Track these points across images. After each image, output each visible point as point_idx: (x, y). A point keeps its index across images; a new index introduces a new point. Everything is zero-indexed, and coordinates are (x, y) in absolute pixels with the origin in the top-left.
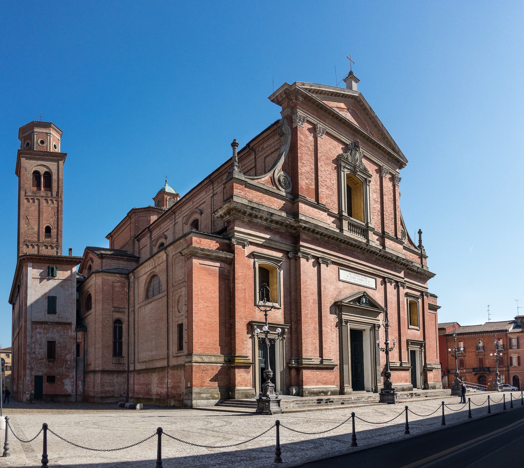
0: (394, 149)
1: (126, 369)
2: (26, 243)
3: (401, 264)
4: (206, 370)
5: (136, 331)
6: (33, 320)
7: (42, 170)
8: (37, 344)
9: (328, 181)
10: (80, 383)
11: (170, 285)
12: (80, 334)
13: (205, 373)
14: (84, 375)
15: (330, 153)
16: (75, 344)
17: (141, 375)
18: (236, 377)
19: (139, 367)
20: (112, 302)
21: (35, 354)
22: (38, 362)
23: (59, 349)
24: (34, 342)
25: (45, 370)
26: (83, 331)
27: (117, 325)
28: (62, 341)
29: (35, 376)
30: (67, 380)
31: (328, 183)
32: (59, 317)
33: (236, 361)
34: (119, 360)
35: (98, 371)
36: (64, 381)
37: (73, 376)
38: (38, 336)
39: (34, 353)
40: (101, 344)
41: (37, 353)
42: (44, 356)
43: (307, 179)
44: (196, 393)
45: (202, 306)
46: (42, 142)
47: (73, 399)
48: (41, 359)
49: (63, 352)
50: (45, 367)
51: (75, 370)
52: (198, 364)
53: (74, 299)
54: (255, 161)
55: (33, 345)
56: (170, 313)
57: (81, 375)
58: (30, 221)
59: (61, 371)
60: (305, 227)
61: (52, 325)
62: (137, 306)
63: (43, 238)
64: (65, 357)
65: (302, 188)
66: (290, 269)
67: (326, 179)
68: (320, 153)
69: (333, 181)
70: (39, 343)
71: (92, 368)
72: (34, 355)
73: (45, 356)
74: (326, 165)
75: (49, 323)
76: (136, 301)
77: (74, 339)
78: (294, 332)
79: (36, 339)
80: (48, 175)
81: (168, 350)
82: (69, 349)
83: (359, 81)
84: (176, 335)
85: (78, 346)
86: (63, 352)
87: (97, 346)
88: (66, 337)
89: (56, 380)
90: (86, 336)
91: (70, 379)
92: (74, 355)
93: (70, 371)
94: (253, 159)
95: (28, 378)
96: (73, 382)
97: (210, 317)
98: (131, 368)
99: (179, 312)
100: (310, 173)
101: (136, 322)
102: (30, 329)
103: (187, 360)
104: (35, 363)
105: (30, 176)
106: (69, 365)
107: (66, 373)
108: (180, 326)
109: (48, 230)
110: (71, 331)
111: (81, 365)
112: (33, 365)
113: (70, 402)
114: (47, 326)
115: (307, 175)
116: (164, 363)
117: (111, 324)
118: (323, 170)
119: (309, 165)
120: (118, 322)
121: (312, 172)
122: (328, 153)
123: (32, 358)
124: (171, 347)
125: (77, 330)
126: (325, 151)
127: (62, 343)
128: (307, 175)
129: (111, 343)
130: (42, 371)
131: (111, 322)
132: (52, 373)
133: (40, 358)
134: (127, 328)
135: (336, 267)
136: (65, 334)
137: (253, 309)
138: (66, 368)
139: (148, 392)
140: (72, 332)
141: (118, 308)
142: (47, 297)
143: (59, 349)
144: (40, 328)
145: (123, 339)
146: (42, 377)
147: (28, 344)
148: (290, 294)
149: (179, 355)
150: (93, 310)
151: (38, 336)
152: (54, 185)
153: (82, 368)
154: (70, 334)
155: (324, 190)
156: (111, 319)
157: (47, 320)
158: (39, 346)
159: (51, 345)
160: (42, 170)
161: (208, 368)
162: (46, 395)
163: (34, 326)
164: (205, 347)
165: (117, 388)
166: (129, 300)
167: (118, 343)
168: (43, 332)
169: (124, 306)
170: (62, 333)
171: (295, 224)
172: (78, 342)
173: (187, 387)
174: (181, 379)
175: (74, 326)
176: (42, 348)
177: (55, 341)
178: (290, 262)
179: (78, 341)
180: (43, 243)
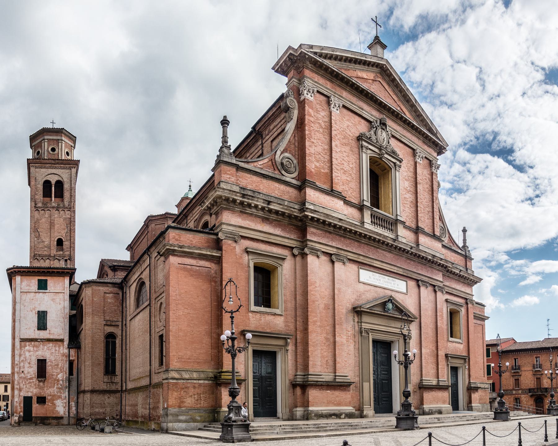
1: (120, 389)
2: (36, 257)
4: (186, 388)
5: (128, 346)
6: (22, 337)
7: (53, 179)
8: (27, 363)
9: (346, 164)
10: (73, 404)
11: (153, 291)
12: (73, 352)
13: (185, 391)
14: (78, 396)
15: (348, 131)
16: (68, 362)
17: (131, 395)
18: (223, 396)
19: (130, 386)
20: (103, 314)
21: (24, 374)
22: (28, 382)
23: (50, 367)
24: (23, 361)
25: (34, 391)
26: (76, 348)
27: (110, 340)
28: (54, 359)
29: (24, 397)
30: (59, 400)
31: (346, 167)
32: (50, 334)
33: (223, 377)
34: (111, 378)
35: (88, 391)
36: (56, 402)
37: (65, 397)
38: (27, 354)
39: (23, 372)
40: (91, 361)
41: (26, 372)
42: (34, 376)
43: (318, 161)
44: (172, 415)
45: (182, 313)
46: (53, 150)
47: (65, 421)
48: (31, 379)
49: (55, 371)
50: (35, 387)
51: (67, 390)
52: (175, 381)
53: (67, 314)
54: (262, 147)
55: (22, 364)
56: (153, 323)
57: (74, 396)
58: (41, 234)
59: (52, 391)
60: (313, 218)
61: (42, 341)
62: (129, 318)
63: (54, 252)
64: (57, 376)
65: (311, 172)
66: (295, 269)
67: (343, 162)
68: (335, 130)
70: (29, 361)
71: (82, 388)
72: (23, 375)
73: (35, 376)
74: (343, 145)
75: (39, 340)
76: (128, 312)
77: (66, 356)
79: (25, 358)
80: (59, 184)
81: (150, 365)
82: (61, 367)
84: (158, 349)
85: (71, 363)
86: (55, 371)
87: (87, 363)
88: (58, 355)
89: (47, 401)
90: (79, 353)
91: (62, 400)
92: (66, 373)
93: (62, 391)
94: (260, 145)
95: (16, 399)
96: (65, 403)
97: (191, 325)
98: (124, 388)
99: (161, 322)
100: (322, 154)
101: (128, 336)
102: (18, 347)
103: (164, 377)
104: (24, 383)
105: (40, 186)
106: (61, 385)
107: (57, 393)
108: (161, 337)
109: (60, 242)
110: (63, 348)
111: (74, 384)
112: (21, 385)
113: (63, 425)
114: (37, 343)
115: (317, 157)
116: (145, 382)
117: (102, 338)
118: (338, 150)
119: (321, 144)
120: (110, 338)
121: (324, 153)
122: (346, 131)
123: (21, 378)
124: (153, 362)
125: (69, 348)
126: (342, 129)
127: (53, 361)
128: (317, 157)
129: (103, 360)
130: (32, 391)
131: (103, 337)
132: (42, 393)
133: (29, 377)
134: (121, 343)
136: (57, 352)
137: (246, 316)
138: (58, 388)
139: (136, 415)
140: (64, 349)
141: (111, 321)
142: (37, 312)
143: (50, 367)
144: (29, 345)
145: (117, 356)
146: (31, 398)
147: (16, 362)
148: (295, 298)
149: (160, 371)
150: (84, 324)
151: (27, 354)
152: (66, 194)
153: (75, 388)
154: (62, 352)
155: (339, 175)
156: (103, 334)
157: (37, 337)
158: (28, 365)
159: (42, 364)
160: (53, 179)
161: (189, 385)
162: (36, 417)
163: (23, 343)
164: (185, 362)
165: (108, 409)
166: (122, 312)
167: (110, 360)
168: (32, 350)
169: (117, 319)
170: (54, 351)
171: (300, 214)
172: (71, 360)
173: (164, 408)
174: (160, 398)
175: (66, 343)
176: (32, 367)
177: (46, 360)
178: (295, 260)
179: (71, 358)
180: (54, 256)
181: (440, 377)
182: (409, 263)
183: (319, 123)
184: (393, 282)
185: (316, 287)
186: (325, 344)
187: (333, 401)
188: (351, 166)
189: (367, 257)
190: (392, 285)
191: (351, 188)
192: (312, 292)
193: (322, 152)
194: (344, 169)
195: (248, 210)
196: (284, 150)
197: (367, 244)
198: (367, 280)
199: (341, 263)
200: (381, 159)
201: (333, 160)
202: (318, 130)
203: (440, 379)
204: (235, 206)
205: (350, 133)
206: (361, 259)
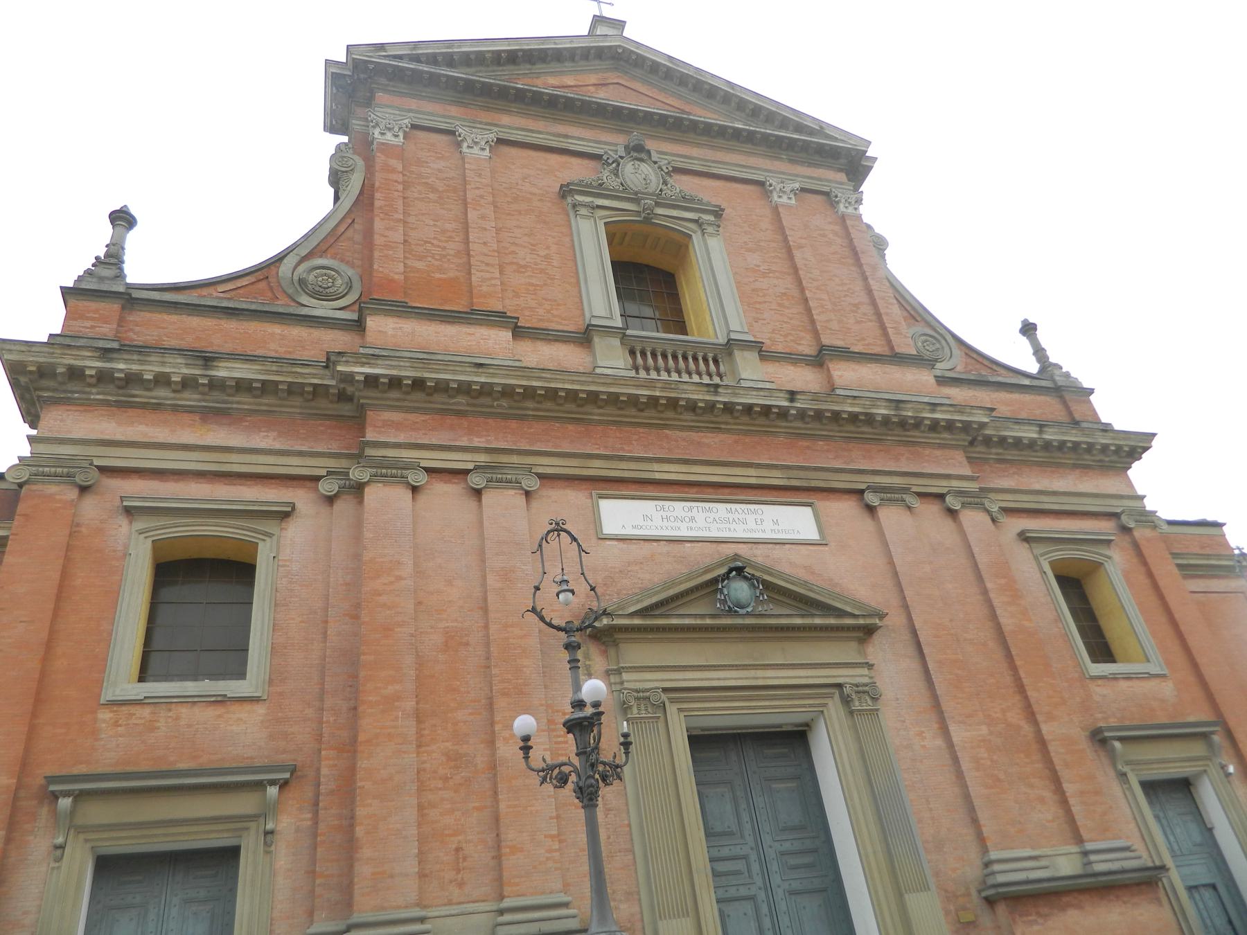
69: (548, 248)
74: (509, 214)
100: (435, 242)
119: (432, 223)
122: (520, 187)
181: (1085, 834)
182: (808, 447)
183: (427, 183)
185: (400, 578)
186: (446, 779)
188: (542, 253)
189: (621, 458)
190: (752, 525)
191: (546, 300)
192: (383, 599)
193: (435, 238)
195: (140, 395)
197: (614, 423)
199: (512, 492)
200: (647, 220)
202: (423, 196)
203: (1089, 846)
204: (88, 389)
206: (597, 468)
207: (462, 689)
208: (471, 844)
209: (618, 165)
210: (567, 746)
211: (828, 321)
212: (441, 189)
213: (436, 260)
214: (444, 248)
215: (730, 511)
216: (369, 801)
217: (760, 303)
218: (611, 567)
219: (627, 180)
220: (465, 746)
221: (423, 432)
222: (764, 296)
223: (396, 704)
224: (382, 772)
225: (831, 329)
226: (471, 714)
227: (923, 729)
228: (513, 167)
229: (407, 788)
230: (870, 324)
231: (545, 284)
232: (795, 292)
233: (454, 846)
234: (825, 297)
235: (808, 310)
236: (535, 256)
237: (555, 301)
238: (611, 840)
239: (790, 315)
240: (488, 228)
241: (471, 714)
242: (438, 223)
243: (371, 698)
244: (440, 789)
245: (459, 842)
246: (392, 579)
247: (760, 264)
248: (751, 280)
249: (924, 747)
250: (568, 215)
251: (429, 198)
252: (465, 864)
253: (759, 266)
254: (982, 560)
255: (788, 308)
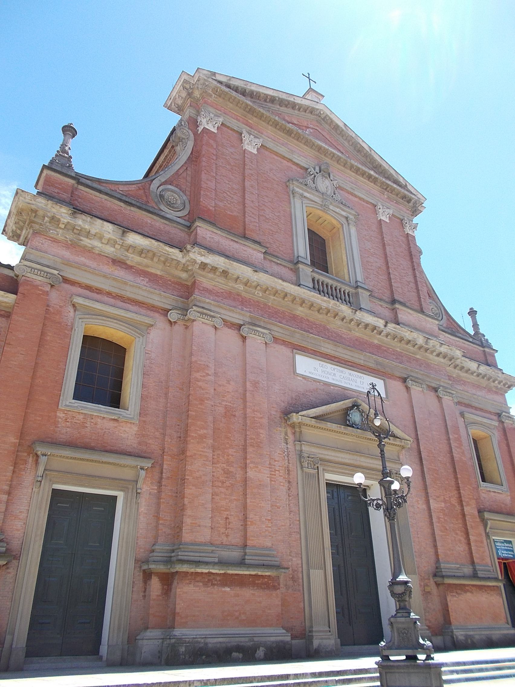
0: (396, 182)
3: (438, 355)
74: (262, 188)
78: (168, 478)
83: (323, 96)
100: (228, 193)
119: (227, 182)
122: (268, 174)
135: (285, 351)
183: (225, 158)
184: (359, 380)
185: (208, 374)
187: (237, 614)
192: (200, 384)
193: (229, 191)
194: (265, 217)
196: (166, 181)
198: (310, 373)
201: (247, 201)
205: (275, 178)
207: (232, 438)
208: (232, 517)
209: (315, 176)
210: (275, 477)
211: (397, 287)
212: (232, 164)
213: (229, 204)
214: (232, 198)
215: (350, 374)
216: (190, 487)
217: (369, 269)
218: (299, 391)
219: (318, 186)
220: (232, 468)
221: (221, 298)
222: (372, 266)
223: (204, 440)
224: (197, 473)
225: (398, 292)
226: (235, 452)
227: (419, 499)
228: (265, 162)
229: (207, 484)
230: (413, 293)
231: (277, 232)
232: (384, 268)
233: (225, 516)
234: (397, 274)
235: (390, 279)
236: (274, 215)
237: (281, 242)
238: (291, 526)
239: (382, 280)
240: (254, 193)
241: (235, 452)
242: (230, 183)
243: (192, 434)
244: (220, 487)
245: (227, 515)
246: (205, 374)
247: (371, 248)
248: (367, 256)
249: (418, 507)
250: (289, 196)
251: (226, 167)
252: (229, 526)
253: (370, 249)
254: (449, 423)
255: (381, 275)
